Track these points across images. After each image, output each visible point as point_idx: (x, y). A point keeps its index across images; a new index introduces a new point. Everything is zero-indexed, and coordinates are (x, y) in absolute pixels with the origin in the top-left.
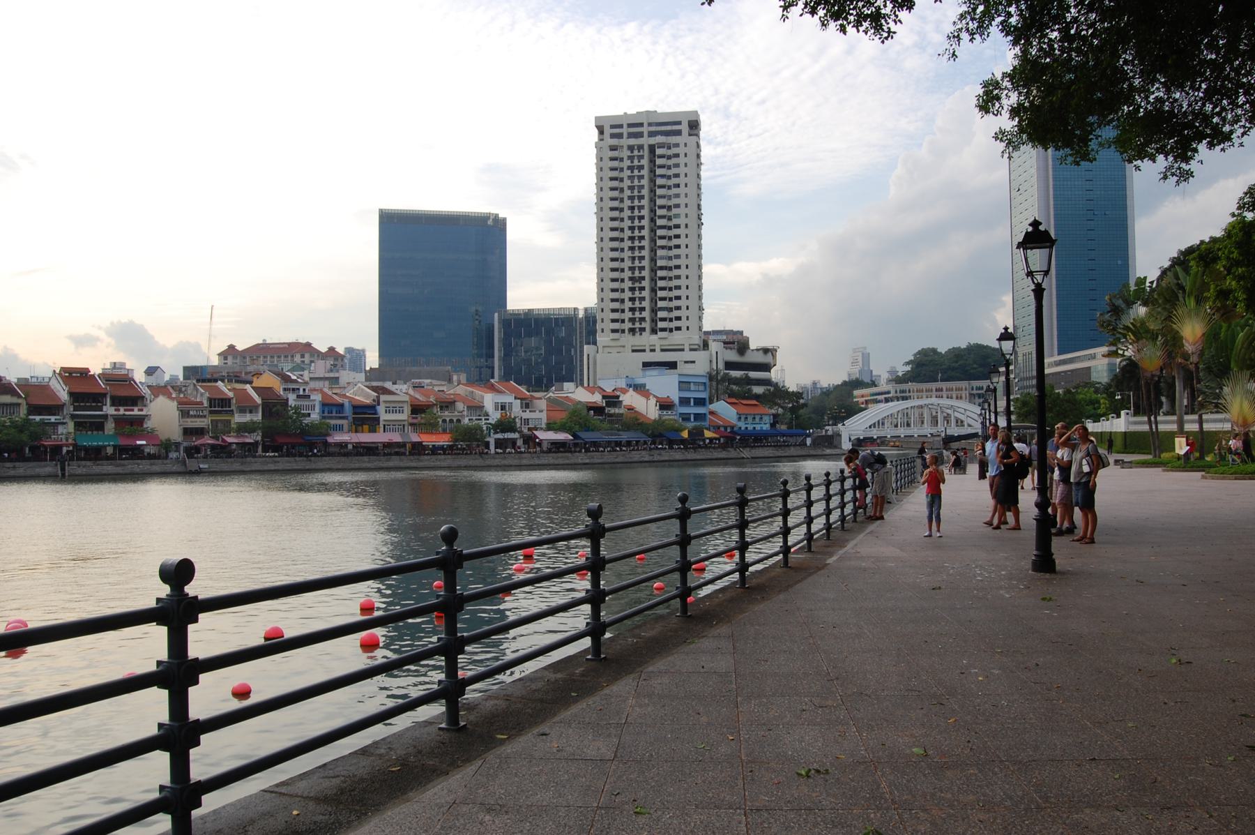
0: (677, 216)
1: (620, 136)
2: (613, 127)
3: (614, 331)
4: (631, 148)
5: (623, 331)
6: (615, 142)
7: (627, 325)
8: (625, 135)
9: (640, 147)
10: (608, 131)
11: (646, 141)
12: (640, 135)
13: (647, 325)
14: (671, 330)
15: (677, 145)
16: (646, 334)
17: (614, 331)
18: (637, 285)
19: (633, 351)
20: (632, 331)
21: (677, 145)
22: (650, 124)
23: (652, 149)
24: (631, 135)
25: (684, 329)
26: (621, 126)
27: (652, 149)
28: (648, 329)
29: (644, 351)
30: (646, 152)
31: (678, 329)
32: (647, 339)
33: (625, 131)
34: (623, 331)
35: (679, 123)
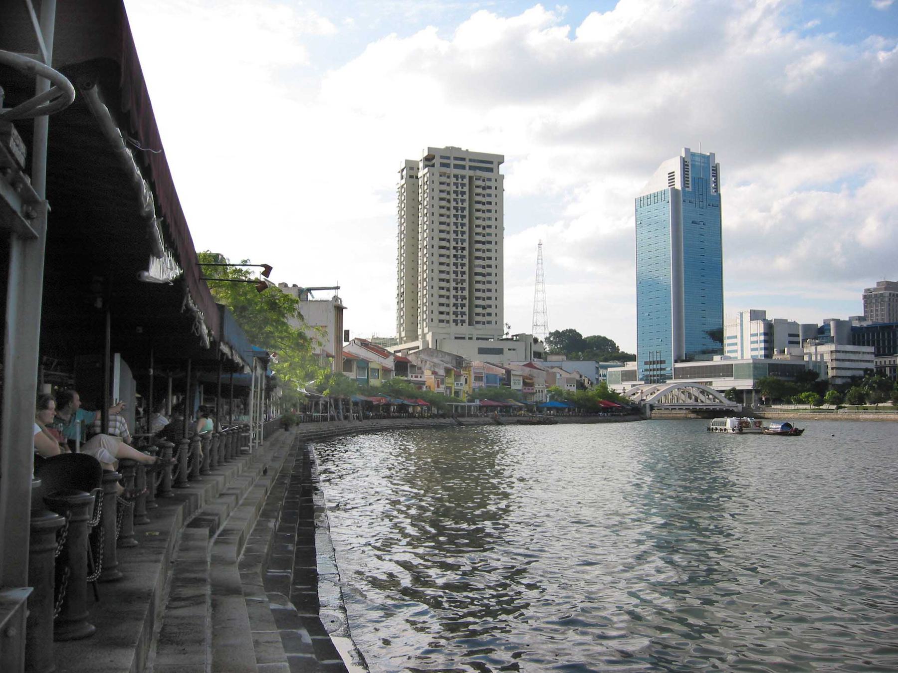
0: (489, 235)
1: (447, 165)
2: (442, 157)
3: (441, 321)
4: (456, 176)
5: (448, 322)
6: (444, 170)
7: (453, 317)
8: (452, 166)
9: (463, 177)
10: (437, 161)
11: (467, 173)
12: (463, 167)
13: (466, 318)
14: (484, 323)
15: (490, 180)
16: (466, 325)
17: (441, 321)
18: (459, 285)
19: (456, 338)
20: (455, 321)
21: (490, 180)
22: (470, 160)
23: (471, 178)
24: (456, 166)
25: (493, 322)
26: (448, 158)
27: (471, 178)
28: (467, 321)
29: (464, 338)
30: (466, 181)
31: (489, 322)
32: (465, 329)
33: (453, 162)
34: (448, 322)
35: (491, 163)
